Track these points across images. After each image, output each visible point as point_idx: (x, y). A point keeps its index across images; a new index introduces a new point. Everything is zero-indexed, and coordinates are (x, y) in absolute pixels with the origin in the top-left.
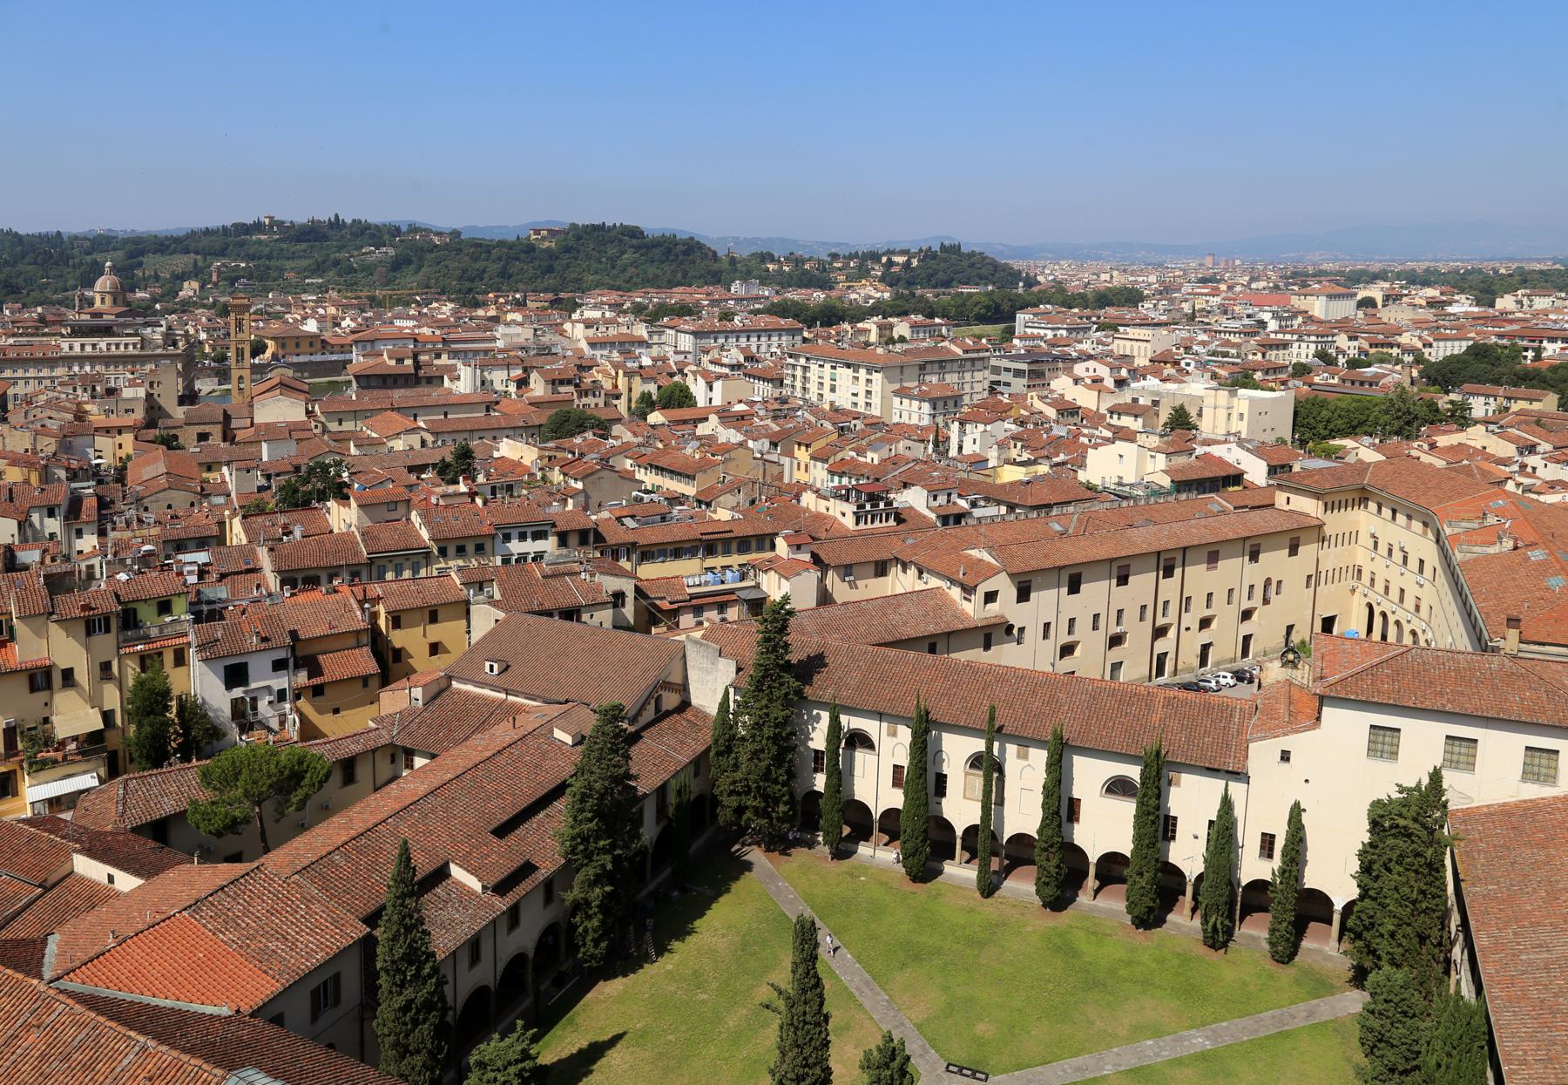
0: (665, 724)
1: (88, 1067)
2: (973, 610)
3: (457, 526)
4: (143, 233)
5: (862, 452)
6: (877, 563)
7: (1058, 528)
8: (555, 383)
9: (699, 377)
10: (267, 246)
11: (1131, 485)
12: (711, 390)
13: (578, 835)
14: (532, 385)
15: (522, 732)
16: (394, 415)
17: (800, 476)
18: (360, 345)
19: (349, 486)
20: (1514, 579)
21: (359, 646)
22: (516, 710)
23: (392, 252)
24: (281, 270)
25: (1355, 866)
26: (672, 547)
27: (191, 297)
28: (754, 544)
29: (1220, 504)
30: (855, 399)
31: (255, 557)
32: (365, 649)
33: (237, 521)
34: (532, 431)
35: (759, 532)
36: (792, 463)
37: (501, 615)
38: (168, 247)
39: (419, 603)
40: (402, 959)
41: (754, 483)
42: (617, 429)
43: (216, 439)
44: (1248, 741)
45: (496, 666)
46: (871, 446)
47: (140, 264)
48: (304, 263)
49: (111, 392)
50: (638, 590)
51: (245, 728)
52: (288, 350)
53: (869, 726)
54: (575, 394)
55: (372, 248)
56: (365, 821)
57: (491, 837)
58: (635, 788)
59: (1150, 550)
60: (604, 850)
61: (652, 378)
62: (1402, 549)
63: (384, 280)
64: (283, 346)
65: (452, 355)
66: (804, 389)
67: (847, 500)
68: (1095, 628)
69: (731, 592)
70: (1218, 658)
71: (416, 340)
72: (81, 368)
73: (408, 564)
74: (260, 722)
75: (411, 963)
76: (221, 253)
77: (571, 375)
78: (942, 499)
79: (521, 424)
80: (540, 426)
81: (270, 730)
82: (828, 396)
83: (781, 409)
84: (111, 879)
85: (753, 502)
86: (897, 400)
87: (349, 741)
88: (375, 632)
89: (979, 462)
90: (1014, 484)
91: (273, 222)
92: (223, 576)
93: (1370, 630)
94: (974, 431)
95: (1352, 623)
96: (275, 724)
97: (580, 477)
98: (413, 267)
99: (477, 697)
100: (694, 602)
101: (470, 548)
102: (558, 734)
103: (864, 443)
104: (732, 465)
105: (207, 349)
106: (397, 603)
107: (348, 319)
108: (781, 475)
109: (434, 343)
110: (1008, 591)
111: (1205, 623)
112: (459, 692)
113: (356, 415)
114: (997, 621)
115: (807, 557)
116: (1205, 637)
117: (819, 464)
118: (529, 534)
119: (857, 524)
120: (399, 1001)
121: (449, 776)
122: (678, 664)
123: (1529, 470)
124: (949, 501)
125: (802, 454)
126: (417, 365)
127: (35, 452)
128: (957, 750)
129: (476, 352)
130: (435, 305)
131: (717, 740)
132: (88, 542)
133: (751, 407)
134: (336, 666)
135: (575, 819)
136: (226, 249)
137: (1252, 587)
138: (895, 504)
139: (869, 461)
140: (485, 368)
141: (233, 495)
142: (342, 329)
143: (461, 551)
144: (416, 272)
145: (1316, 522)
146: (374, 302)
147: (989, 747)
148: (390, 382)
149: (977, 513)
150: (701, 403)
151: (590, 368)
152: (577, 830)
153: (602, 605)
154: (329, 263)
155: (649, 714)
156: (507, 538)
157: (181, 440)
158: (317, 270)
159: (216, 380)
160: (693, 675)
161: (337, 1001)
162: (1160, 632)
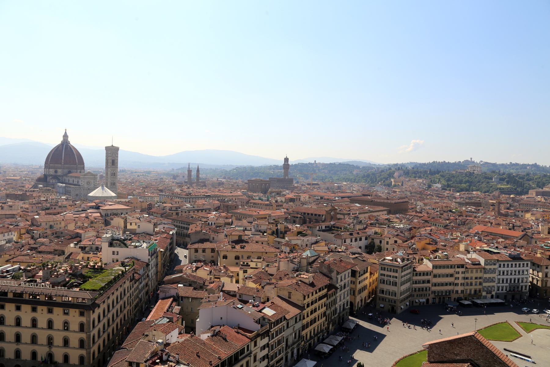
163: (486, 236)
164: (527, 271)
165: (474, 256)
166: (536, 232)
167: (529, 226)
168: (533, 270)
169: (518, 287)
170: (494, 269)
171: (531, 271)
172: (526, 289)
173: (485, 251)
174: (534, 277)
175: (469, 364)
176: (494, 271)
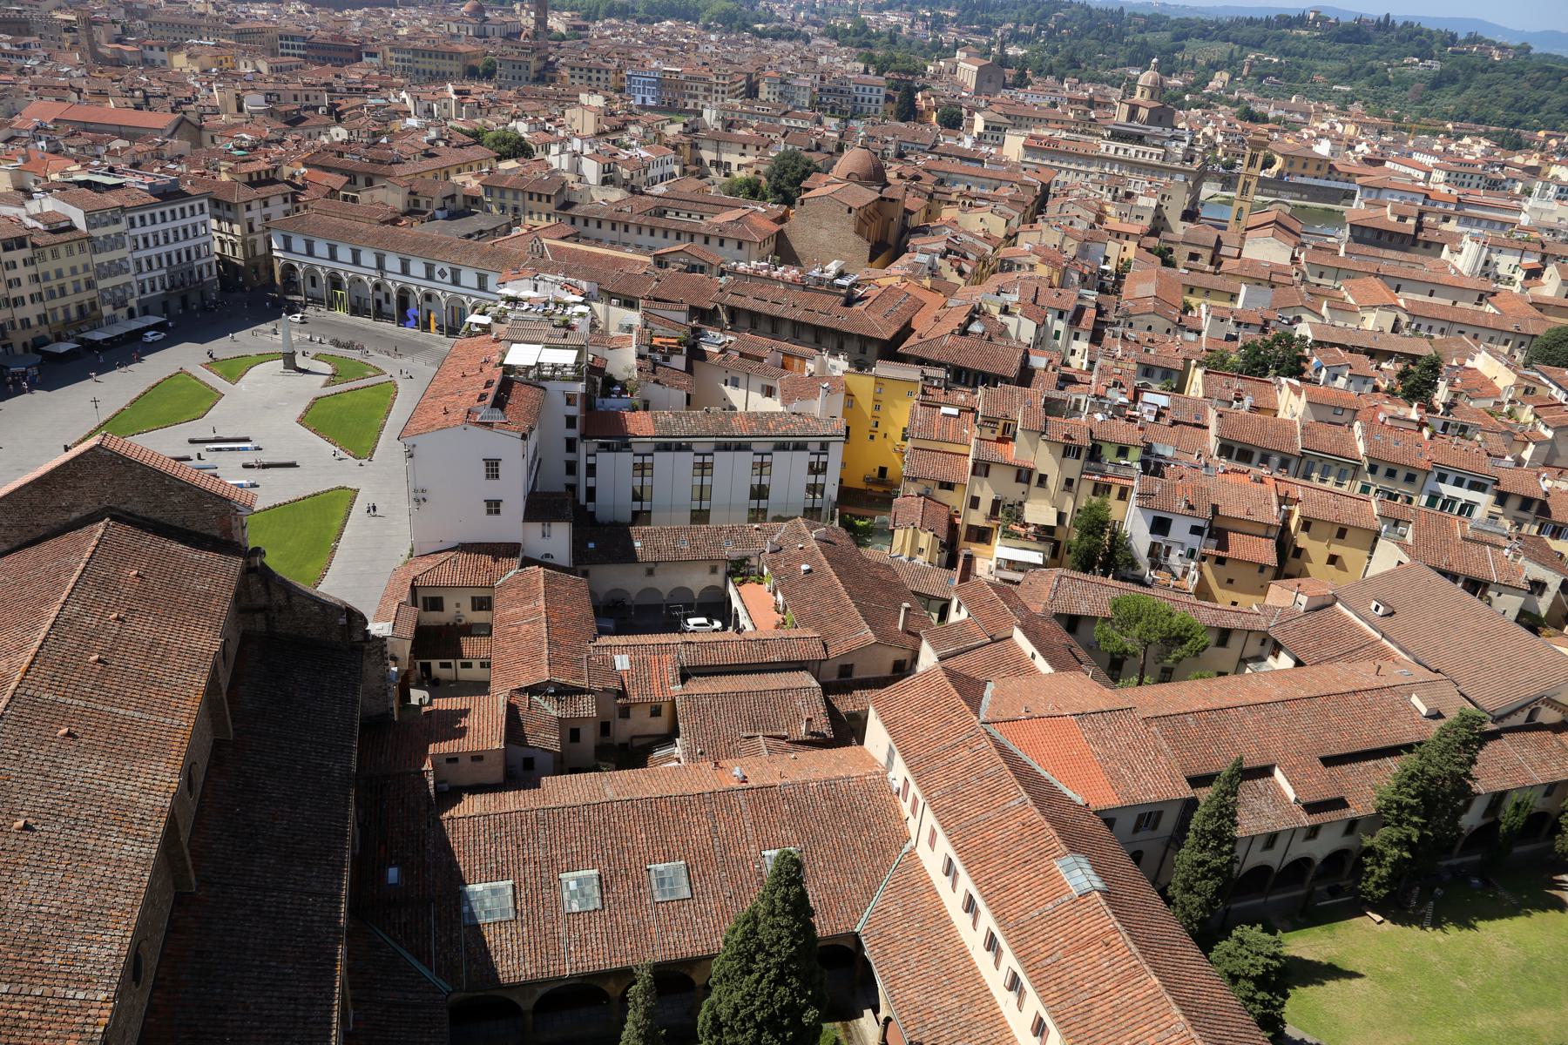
1: (991, 792)
3: (1397, 449)
4: (1192, 9)
10: (1305, 42)
13: (1397, 802)
14: (1544, 279)
16: (1376, 282)
18: (1366, 190)
19: (1307, 361)
22: (1386, 655)
23: (1437, 66)
24: (1312, 69)
27: (1219, 89)
31: (1205, 415)
33: (1199, 372)
37: (1406, 560)
38: (1211, 32)
43: (1204, 263)
45: (1381, 609)
47: (1182, 48)
48: (1336, 66)
49: (1129, 195)
51: (1155, 566)
52: (1293, 170)
55: (1416, 60)
57: (1319, 762)
63: (1418, 97)
64: (1291, 164)
65: (1462, 220)
71: (1427, 196)
72: (1111, 168)
73: (1335, 469)
75: (1215, 837)
76: (1258, 45)
81: (1174, 575)
84: (1033, 656)
87: (1232, 614)
91: (1318, 18)
92: (1175, 423)
96: (1179, 572)
97: (1553, 425)
98: (1456, 87)
99: (1353, 625)
101: (1401, 475)
102: (1415, 700)
105: (1220, 153)
106: (1312, 512)
107: (1364, 144)
109: (1446, 204)
112: (1340, 614)
113: (1339, 273)
118: (1466, 483)
120: (1199, 857)
121: (1302, 693)
126: (1419, 227)
127: (1061, 247)
129: (1491, 223)
130: (1467, 140)
132: (1082, 345)
134: (1241, 547)
135: (1399, 787)
136: (1264, 41)
140: (1495, 249)
141: (1204, 335)
142: (1354, 153)
143: (1391, 474)
144: (1458, 94)
146: (1398, 126)
148: (1384, 238)
152: (1396, 797)
154: (1364, 70)
156: (1442, 478)
157: (1175, 255)
158: (1349, 76)
159: (1220, 185)
161: (1155, 827)
163: (72, 135)
164: (204, 224)
165: (50, 204)
166: (208, 110)
167: (188, 94)
168: (219, 222)
169: (191, 273)
170: (118, 234)
171: (214, 223)
172: (211, 274)
173: (81, 184)
174: (224, 236)
175: (107, 519)
176: (117, 242)
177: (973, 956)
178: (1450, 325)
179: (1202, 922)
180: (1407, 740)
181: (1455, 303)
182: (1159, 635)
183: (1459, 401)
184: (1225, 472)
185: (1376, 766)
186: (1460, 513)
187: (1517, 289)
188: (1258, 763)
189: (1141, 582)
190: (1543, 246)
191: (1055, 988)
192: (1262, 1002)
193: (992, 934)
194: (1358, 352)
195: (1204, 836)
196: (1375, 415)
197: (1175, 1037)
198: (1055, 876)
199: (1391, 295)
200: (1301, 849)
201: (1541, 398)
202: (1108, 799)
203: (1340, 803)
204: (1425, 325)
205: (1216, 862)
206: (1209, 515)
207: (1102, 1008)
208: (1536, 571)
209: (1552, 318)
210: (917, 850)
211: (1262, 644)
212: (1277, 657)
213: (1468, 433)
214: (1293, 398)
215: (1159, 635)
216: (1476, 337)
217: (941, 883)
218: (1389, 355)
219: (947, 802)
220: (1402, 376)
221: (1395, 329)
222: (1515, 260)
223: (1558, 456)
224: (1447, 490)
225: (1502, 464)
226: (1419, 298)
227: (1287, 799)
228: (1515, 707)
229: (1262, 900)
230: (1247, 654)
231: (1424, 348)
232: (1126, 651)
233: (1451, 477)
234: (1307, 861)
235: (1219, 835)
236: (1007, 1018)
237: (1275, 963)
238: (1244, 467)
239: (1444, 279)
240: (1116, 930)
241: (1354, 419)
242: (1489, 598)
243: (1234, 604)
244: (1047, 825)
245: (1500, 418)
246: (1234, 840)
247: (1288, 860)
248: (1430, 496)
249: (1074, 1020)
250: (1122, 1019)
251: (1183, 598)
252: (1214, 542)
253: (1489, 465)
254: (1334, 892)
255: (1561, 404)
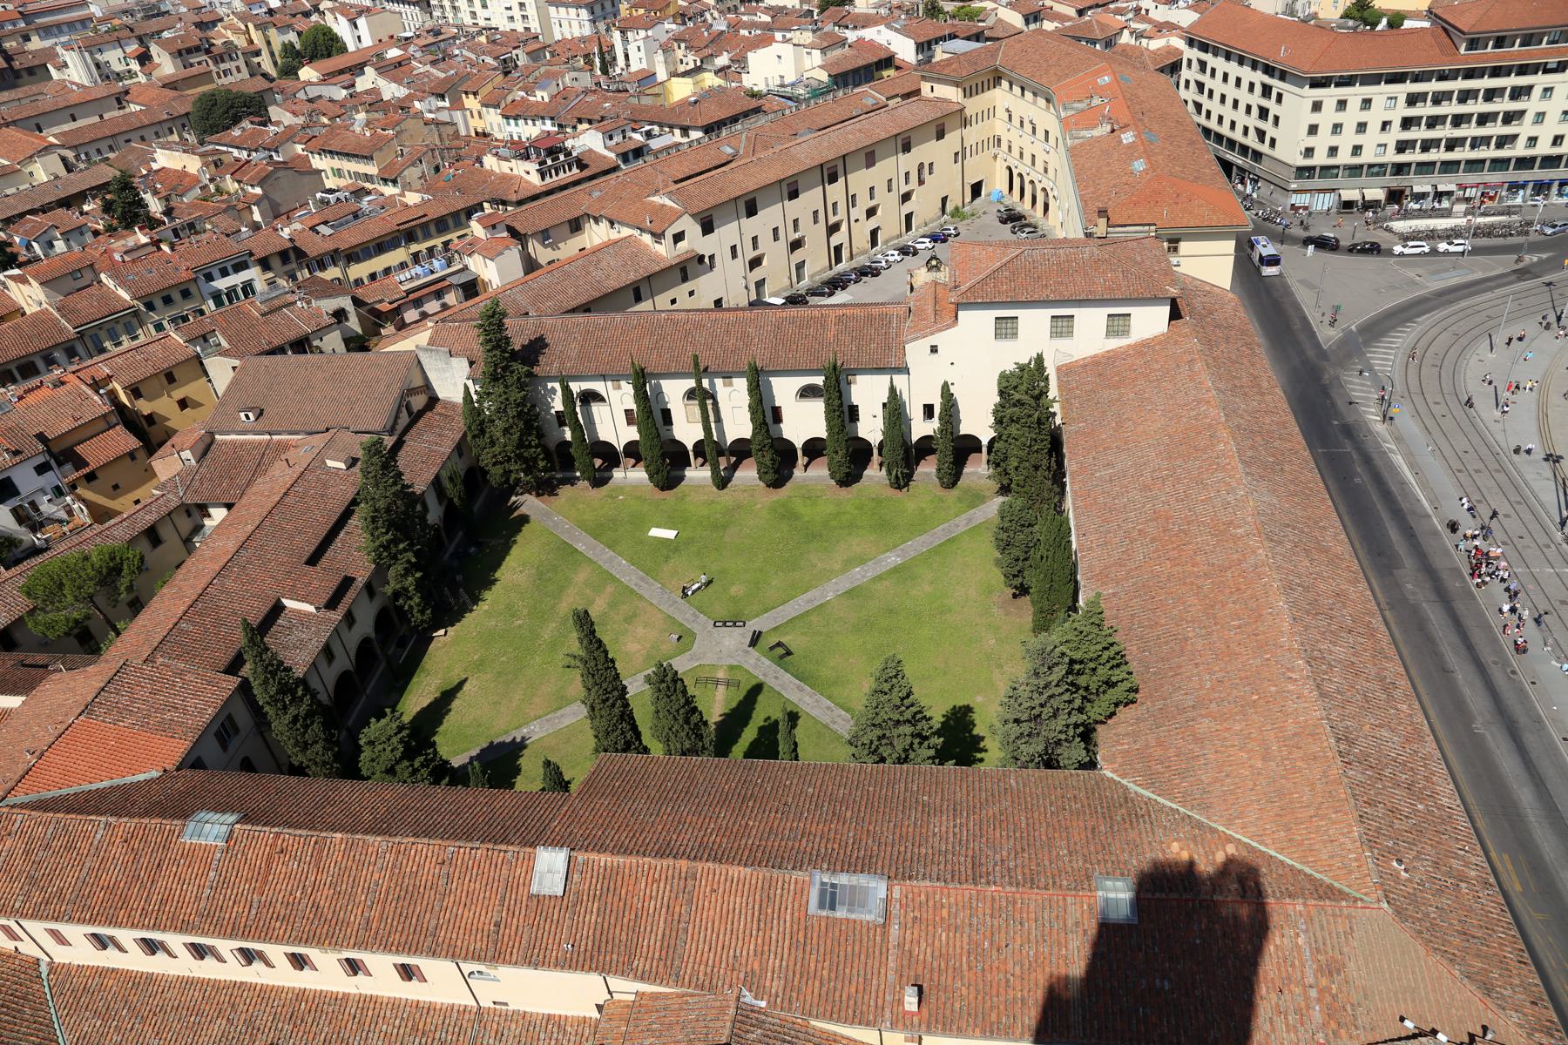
0: (421, 423)
2: (665, 251)
3: (154, 277)
5: (529, 91)
6: (570, 221)
7: (729, 150)
8: (182, 54)
9: (338, 15)
11: (793, 85)
12: (356, 27)
14: (156, 60)
15: (299, 469)
17: (476, 124)
20: (1109, 164)
21: (111, 427)
22: (284, 447)
25: (992, 420)
26: (371, 245)
28: (451, 222)
29: (873, 97)
30: (510, 13)
32: (118, 428)
34: (179, 123)
35: (453, 210)
36: (465, 117)
37: (236, 363)
39: (152, 371)
40: (277, 693)
41: (433, 150)
42: (274, 112)
44: (905, 342)
45: (250, 415)
46: (538, 84)
50: (357, 302)
51: (35, 527)
53: (598, 386)
54: (210, 62)
56: (192, 587)
57: (307, 568)
58: (413, 493)
59: (813, 164)
60: (405, 550)
61: (288, 26)
62: (1031, 122)
66: (454, 8)
67: (528, 158)
68: (776, 238)
69: (443, 279)
70: (886, 237)
73: (119, 327)
74: (48, 519)
75: (284, 693)
77: (195, 37)
78: (618, 138)
79: (166, 117)
80: (187, 114)
81: (61, 521)
82: (481, 13)
83: (437, 44)
85: (437, 169)
86: (552, 10)
87: (141, 513)
88: (119, 407)
89: (648, 78)
90: (684, 103)
93: (1011, 188)
94: (637, 38)
95: (997, 184)
96: (63, 515)
99: (243, 444)
100: (412, 296)
101: (176, 296)
102: (330, 463)
103: (530, 79)
104: (405, 136)
108: (456, 134)
110: (692, 228)
111: (871, 212)
112: (225, 443)
114: (689, 256)
115: (505, 234)
116: (873, 223)
117: (492, 110)
119: (543, 179)
120: (288, 717)
121: (250, 528)
122: (417, 371)
123: (1143, 12)
124: (624, 137)
125: (471, 102)
128: (674, 391)
131: (470, 427)
133: (405, 50)
134: (96, 452)
135: (372, 535)
137: (907, 174)
138: (574, 154)
139: (540, 99)
140: (94, 49)
143: (168, 300)
145: (958, 107)
147: (699, 382)
149: (655, 144)
150: (351, 47)
151: (214, 23)
152: (377, 543)
153: (327, 328)
155: (404, 419)
156: (209, 278)
160: (432, 376)
161: (237, 731)
162: (833, 229)
177: (197, 975)
178: (116, 138)
179: (337, 757)
180: (350, 497)
181: (101, 117)
182: (92, 583)
183: (173, 204)
184: (20, 398)
185: (347, 533)
186: (246, 297)
187: (142, 79)
188: (265, 609)
189: (35, 551)
190: (132, 30)
191: (278, 924)
192: (422, 765)
193: (193, 945)
194: (51, 209)
195: (277, 701)
196: (111, 259)
197: (388, 855)
198: (194, 849)
199: (37, 137)
200: (353, 638)
201: (232, 165)
202: (178, 748)
203: (347, 582)
204: (92, 152)
205: (303, 709)
206: (41, 447)
207: (323, 897)
208: (329, 305)
209: (189, 92)
210: (56, 960)
211: (189, 515)
212: (209, 516)
213: (198, 227)
214: (24, 288)
215: (92, 583)
216: (143, 138)
217: (109, 959)
218: (81, 197)
219: (37, 897)
220: (107, 208)
221: (69, 168)
222: (119, 53)
223: (279, 205)
224: (222, 284)
225: (243, 236)
226: (66, 127)
227: (309, 614)
228: (394, 414)
229: (364, 699)
230: (185, 532)
231: (107, 173)
232: (76, 622)
233: (216, 272)
234: (365, 644)
235: (285, 689)
236: (271, 983)
237: (405, 733)
238: (35, 381)
239: (73, 99)
240: (278, 835)
241: (97, 275)
242: (317, 347)
243: (137, 502)
244: (146, 821)
245: (214, 199)
246: (303, 682)
247: (353, 654)
248: (213, 298)
249: (314, 927)
250: (344, 886)
251: (88, 534)
252: (68, 467)
253: (234, 244)
254: (402, 643)
255: (248, 162)
